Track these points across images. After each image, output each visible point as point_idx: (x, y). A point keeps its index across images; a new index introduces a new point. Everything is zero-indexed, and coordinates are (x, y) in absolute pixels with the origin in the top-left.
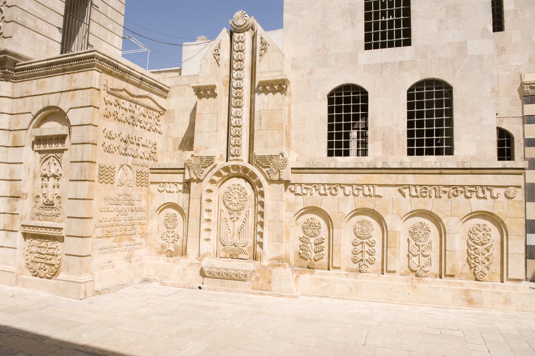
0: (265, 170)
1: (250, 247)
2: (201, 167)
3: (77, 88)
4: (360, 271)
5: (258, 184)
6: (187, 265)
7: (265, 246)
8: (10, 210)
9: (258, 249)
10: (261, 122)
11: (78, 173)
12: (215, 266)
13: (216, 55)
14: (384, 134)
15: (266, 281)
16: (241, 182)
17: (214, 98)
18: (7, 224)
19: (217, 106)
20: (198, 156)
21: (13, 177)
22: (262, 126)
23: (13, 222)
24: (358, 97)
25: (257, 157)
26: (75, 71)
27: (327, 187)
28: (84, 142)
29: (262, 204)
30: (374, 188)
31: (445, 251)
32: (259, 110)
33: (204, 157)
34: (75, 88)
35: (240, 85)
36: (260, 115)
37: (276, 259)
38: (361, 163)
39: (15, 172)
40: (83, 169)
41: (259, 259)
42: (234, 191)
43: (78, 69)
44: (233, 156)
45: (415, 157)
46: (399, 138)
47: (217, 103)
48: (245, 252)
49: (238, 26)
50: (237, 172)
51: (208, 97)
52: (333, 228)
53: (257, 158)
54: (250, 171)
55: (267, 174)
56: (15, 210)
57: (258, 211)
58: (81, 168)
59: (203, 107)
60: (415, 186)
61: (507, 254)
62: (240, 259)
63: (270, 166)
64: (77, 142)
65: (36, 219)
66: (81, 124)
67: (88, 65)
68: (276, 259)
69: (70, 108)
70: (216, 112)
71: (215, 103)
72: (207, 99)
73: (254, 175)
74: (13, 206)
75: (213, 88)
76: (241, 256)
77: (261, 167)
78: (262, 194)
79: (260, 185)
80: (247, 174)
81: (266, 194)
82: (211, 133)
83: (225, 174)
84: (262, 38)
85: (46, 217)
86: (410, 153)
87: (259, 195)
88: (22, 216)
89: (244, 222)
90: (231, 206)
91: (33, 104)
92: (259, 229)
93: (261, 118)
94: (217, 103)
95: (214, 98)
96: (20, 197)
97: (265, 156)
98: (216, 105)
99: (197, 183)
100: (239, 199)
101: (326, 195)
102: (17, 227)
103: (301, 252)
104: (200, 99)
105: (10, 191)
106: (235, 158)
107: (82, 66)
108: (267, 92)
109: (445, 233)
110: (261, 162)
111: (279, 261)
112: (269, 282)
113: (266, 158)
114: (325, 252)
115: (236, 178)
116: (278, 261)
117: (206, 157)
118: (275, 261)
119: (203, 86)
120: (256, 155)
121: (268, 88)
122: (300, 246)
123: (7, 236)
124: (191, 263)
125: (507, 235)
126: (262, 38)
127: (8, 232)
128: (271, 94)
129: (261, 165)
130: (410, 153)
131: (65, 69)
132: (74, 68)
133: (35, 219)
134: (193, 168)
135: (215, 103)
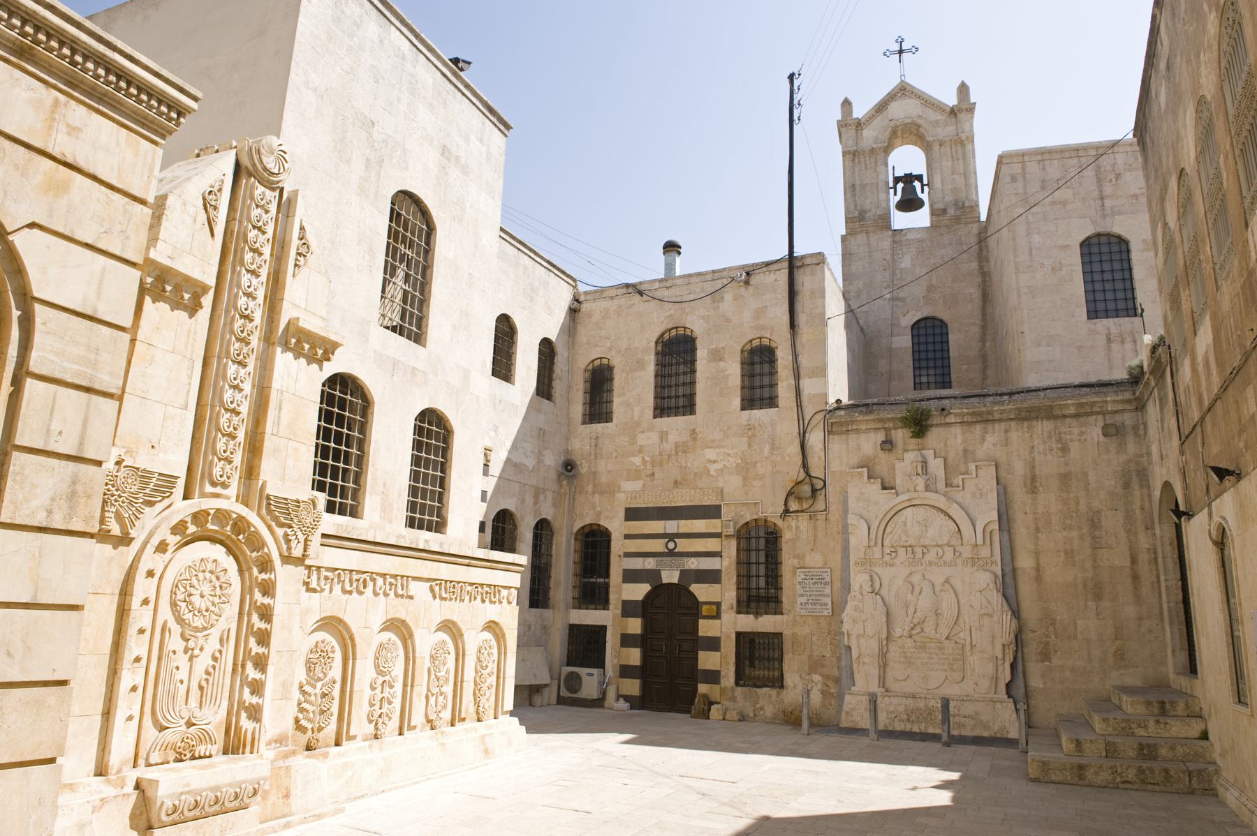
0: (280, 532)
1: (221, 723)
2: (141, 500)
3: (81, 163)
4: (376, 737)
5: (258, 563)
6: (90, 810)
7: (267, 715)
9: (246, 724)
10: (279, 418)
11: (53, 500)
12: (192, 787)
13: (211, 205)
14: (384, 484)
15: (280, 796)
16: (218, 552)
17: (191, 317)
19: (194, 339)
20: (138, 469)
22: (281, 427)
24: (357, 403)
25: (272, 498)
26: (76, 94)
27: (355, 577)
28: (97, 386)
29: (266, 614)
30: (407, 581)
31: (462, 681)
32: (279, 387)
33: (153, 473)
34: (70, 160)
35: (252, 312)
36: (281, 401)
37: (276, 741)
38: (403, 537)
40: (79, 488)
41: (248, 748)
42: (208, 575)
43: (99, 99)
44: (214, 484)
45: (415, 532)
46: (399, 495)
47: (195, 333)
48: (210, 738)
49: (265, 169)
50: (216, 528)
51: (176, 305)
52: (354, 659)
53: (272, 502)
54: (252, 529)
55: (283, 542)
57: (255, 629)
58: (74, 483)
59: (158, 328)
60: (446, 581)
61: (504, 678)
62: (200, 757)
63: (294, 525)
64: (57, 374)
66: (89, 312)
67: (146, 117)
68: (276, 741)
69: (32, 225)
70: (188, 355)
71: (189, 331)
72: (172, 310)
73: (256, 542)
75: (199, 290)
76: (201, 749)
77: (273, 524)
78: (268, 589)
79: (265, 565)
80: (241, 537)
81: (280, 590)
82: (170, 409)
83: (192, 529)
84: (302, 228)
86: (411, 523)
87: (257, 590)
89: (215, 659)
90: (188, 616)
92: (252, 673)
93: (280, 408)
94: (195, 333)
95: (191, 317)
97: (286, 499)
98: (192, 334)
99: (115, 547)
100: (211, 598)
101: (350, 592)
103: (301, 716)
104: (154, 302)
106: (218, 490)
107: (119, 102)
108: (298, 354)
109: (464, 655)
110: (280, 512)
111: (281, 744)
112: (287, 796)
113: (286, 504)
114: (335, 709)
115: (208, 542)
116: (278, 745)
117: (160, 474)
118: (273, 744)
119: (177, 274)
120: (270, 490)
121: (307, 346)
122: (299, 704)
124: (102, 800)
125: (505, 653)
126: (302, 228)
128: (303, 361)
129: (276, 519)
130: (411, 523)
131: (33, 55)
132: (82, 82)
134: (116, 501)
135: (189, 331)
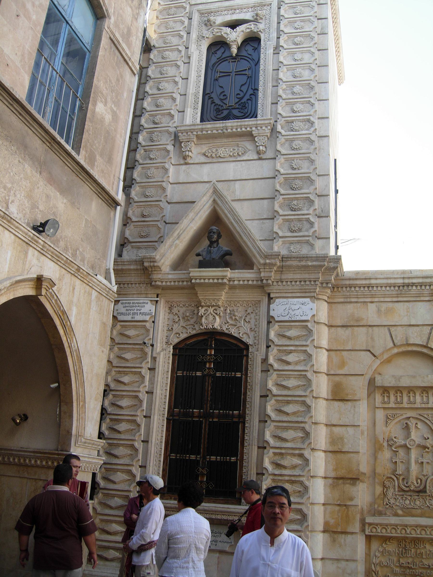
8: (339, 500)
18: (332, 521)
21: (340, 447)
23: (347, 519)
39: (346, 440)
56: (351, 499)
65: (388, 513)
74: (344, 492)
85: (408, 512)
88: (362, 509)
91: (372, 338)
96: (358, 479)
102: (356, 527)
105: (335, 470)
123: (334, 541)
127: (336, 536)
133: (385, 514)
